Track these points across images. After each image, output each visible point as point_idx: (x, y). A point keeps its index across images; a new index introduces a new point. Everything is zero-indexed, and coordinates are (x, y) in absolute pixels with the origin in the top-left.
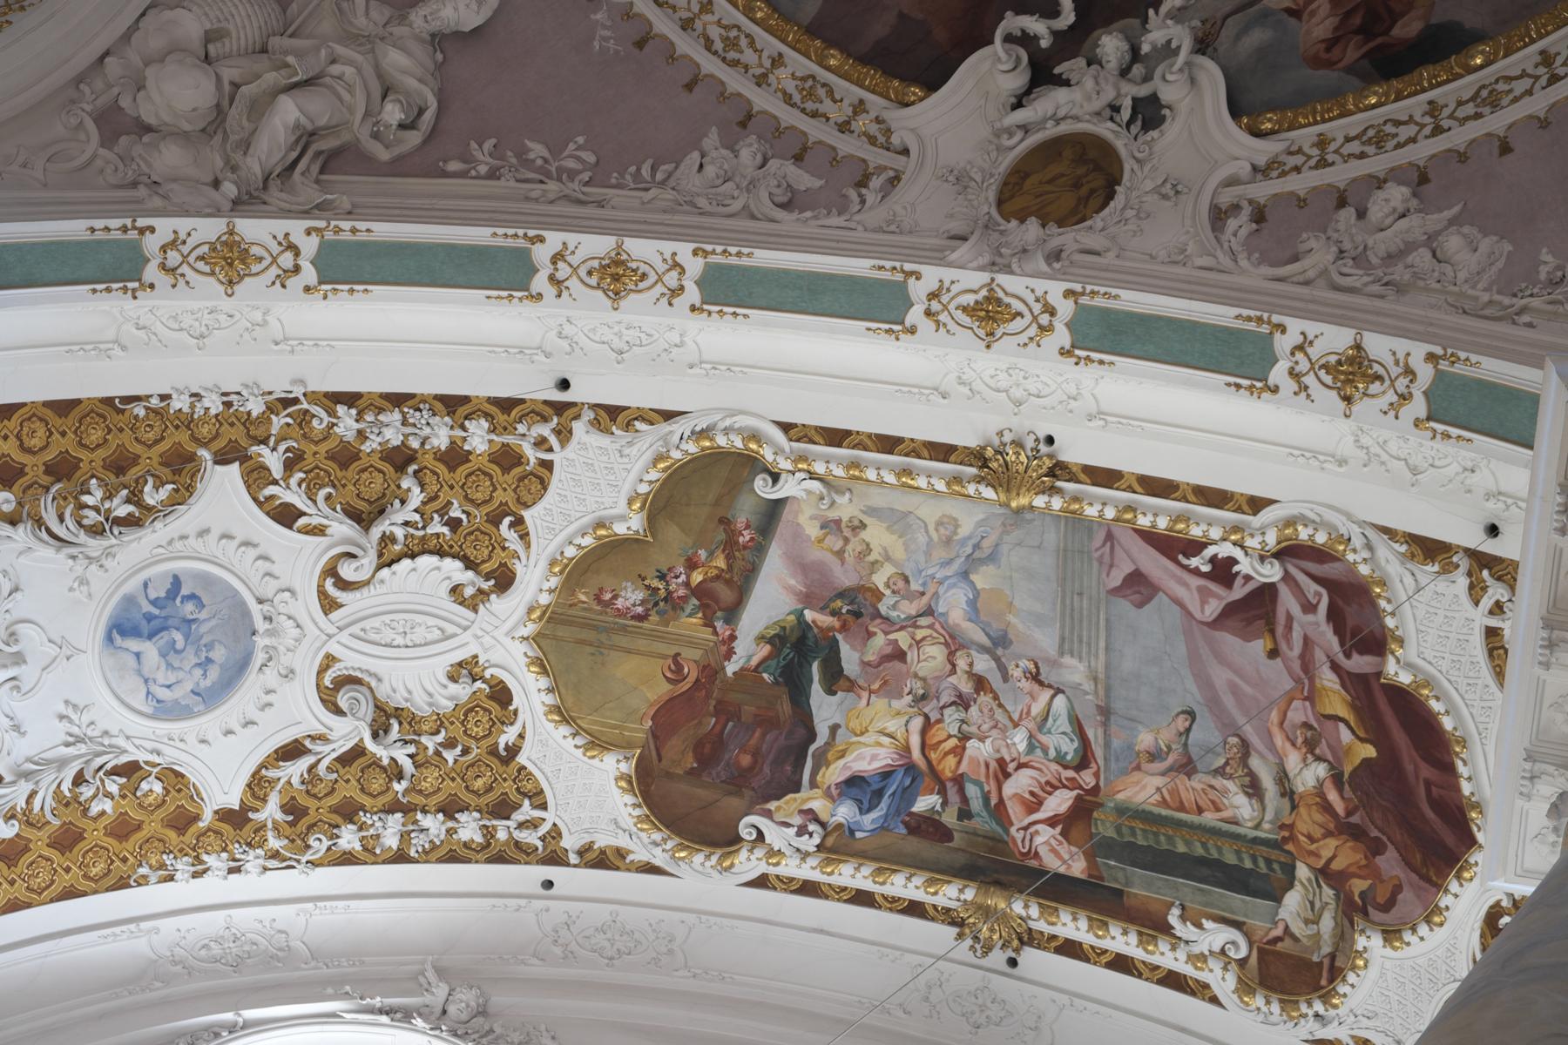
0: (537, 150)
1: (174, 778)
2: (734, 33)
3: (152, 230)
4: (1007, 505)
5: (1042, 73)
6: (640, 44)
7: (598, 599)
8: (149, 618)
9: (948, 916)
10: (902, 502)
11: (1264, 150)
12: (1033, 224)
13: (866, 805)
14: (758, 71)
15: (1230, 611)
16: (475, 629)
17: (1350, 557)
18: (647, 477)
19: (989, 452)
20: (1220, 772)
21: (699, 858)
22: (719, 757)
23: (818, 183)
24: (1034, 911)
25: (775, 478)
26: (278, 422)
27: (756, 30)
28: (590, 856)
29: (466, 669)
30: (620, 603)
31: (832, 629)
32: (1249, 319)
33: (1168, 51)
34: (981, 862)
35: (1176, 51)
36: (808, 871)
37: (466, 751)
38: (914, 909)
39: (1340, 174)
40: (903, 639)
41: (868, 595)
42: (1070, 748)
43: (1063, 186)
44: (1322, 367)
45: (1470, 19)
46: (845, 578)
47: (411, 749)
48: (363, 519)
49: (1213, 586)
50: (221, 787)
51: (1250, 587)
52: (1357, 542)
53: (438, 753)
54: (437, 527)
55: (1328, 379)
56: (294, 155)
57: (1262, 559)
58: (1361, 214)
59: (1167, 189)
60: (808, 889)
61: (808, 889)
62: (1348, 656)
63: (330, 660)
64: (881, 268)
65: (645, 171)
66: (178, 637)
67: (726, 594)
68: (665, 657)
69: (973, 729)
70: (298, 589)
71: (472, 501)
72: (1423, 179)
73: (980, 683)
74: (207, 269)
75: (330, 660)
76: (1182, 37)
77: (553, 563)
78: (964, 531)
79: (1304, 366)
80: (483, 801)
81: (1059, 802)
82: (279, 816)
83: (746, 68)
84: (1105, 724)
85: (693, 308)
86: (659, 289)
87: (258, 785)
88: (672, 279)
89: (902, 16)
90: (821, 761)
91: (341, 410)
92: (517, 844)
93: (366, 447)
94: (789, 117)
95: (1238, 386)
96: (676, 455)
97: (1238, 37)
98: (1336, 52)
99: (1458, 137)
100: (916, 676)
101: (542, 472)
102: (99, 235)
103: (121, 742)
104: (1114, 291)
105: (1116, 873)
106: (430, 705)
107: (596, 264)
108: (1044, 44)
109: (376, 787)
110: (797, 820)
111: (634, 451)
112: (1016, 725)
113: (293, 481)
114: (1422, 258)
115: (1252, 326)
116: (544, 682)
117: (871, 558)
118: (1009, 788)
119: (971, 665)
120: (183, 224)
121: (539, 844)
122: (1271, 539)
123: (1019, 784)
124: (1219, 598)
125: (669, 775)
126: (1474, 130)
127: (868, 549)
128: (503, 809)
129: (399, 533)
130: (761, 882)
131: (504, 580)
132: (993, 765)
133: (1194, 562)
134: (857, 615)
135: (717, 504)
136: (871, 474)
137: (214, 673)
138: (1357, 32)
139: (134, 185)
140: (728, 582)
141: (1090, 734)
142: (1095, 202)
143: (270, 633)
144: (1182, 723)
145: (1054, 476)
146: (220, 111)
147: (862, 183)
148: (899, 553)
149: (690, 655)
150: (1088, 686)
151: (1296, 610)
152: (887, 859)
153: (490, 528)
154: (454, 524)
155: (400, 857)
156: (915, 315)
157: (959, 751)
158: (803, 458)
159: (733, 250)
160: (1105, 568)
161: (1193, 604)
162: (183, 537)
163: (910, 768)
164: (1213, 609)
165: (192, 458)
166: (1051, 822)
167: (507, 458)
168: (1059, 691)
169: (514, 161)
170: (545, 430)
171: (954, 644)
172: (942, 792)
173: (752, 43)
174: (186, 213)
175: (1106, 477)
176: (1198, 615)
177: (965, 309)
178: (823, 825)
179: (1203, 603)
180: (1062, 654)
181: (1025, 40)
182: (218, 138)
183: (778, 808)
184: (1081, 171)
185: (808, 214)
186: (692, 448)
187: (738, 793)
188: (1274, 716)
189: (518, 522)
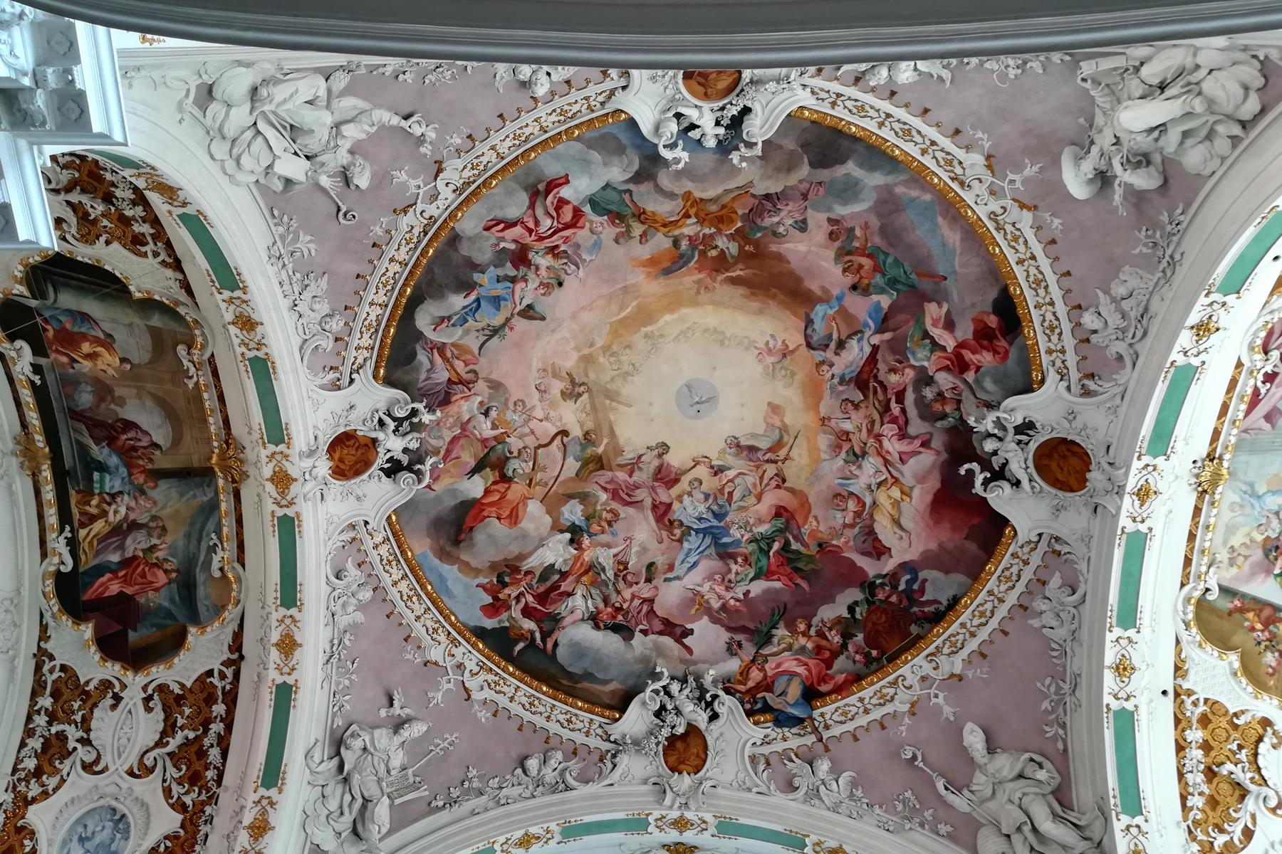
5: (1000, 475)
6: (984, 656)
7: (1272, 675)
10: (1221, 530)
11: (1052, 377)
12: (1088, 475)
23: (1058, 574)
25: (1208, 590)
26: (1201, 837)
27: (976, 603)
30: (1274, 664)
33: (999, 423)
35: (998, 418)
39: (1069, 342)
43: (1064, 464)
45: (993, 294)
46: (1258, 554)
48: (1244, 793)
54: (1243, 755)
59: (1071, 417)
67: (1267, 612)
76: (991, 417)
77: (1256, 698)
79: (1195, 351)
86: (1129, 648)
88: (1124, 642)
93: (1207, 791)
94: (1020, 587)
96: (1198, 638)
97: (988, 392)
101: (1210, 703)
113: (1230, 829)
114: (1126, 305)
115: (1169, 376)
127: (1244, 544)
129: (1249, 775)
131: (1266, 723)
135: (1221, 617)
138: (991, 342)
140: (1261, 611)
142: (1075, 449)
147: (1059, 554)
148: (1246, 530)
153: (1240, 729)
154: (1240, 747)
156: (1143, 528)
158: (1199, 577)
167: (1204, 721)
170: (1188, 702)
173: (982, 605)
177: (1142, 505)
181: (986, 483)
184: (1056, 456)
186: (1194, 630)
189: (1236, 715)
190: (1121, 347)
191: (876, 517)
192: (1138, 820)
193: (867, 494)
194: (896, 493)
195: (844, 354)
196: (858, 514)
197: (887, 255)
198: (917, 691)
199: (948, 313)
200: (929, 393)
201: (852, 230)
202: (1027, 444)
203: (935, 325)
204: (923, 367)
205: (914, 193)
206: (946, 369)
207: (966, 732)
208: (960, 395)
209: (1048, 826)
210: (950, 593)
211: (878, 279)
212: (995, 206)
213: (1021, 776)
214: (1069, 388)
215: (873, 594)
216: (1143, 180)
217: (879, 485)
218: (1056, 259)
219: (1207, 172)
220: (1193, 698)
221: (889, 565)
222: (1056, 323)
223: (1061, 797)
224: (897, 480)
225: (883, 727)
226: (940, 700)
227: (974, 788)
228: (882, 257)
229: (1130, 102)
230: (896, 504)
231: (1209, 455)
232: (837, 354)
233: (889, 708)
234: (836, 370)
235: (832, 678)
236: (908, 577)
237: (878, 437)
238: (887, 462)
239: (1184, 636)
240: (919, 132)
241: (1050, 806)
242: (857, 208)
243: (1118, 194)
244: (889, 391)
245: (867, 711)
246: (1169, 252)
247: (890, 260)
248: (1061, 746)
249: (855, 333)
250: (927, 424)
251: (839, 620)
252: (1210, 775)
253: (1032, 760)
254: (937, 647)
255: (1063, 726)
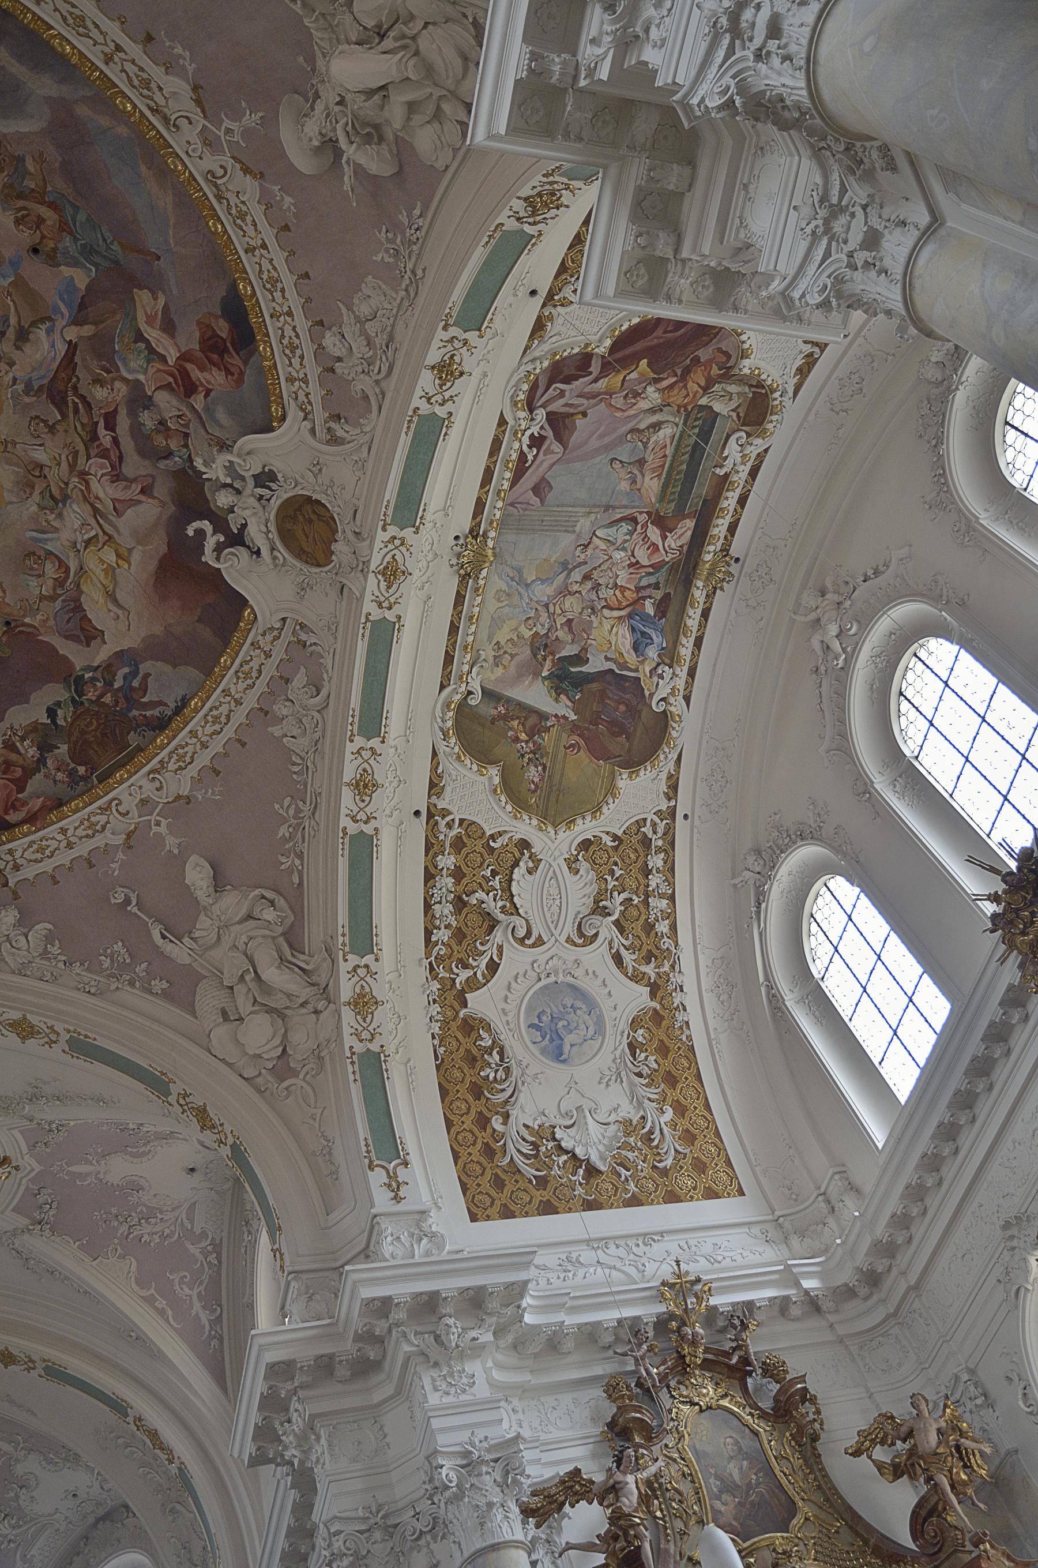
0: (283, 831)
1: (635, 1023)
2: (209, 718)
3: (351, 1047)
4: (492, 562)
5: (237, 539)
6: (217, 773)
7: (534, 792)
8: (552, 1040)
9: (710, 597)
10: (485, 622)
11: (293, 413)
13: (649, 641)
14: (233, 704)
15: (558, 437)
16: (550, 860)
17: (538, 371)
18: (469, 766)
19: (462, 572)
20: (645, 445)
21: (674, 734)
22: (622, 724)
23: (303, 670)
24: (712, 548)
25: (470, 693)
28: (671, 794)
29: (572, 864)
30: (536, 780)
31: (553, 661)
32: (408, 427)
33: (230, 469)
34: (683, 577)
36: (683, 673)
37: (616, 864)
38: (705, 614)
39: (313, 370)
40: (561, 620)
41: (535, 640)
42: (625, 527)
43: (309, 528)
44: (441, 386)
45: (221, 292)
47: (616, 893)
49: (544, 448)
50: (637, 998)
51: (547, 427)
52: (530, 367)
53: (617, 879)
54: (496, 883)
55: (449, 384)
56: (296, 969)
57: (532, 419)
58: (339, 359)
59: (315, 470)
60: (692, 673)
61: (692, 673)
62: (591, 373)
63: (569, 940)
64: (363, 636)
65: (296, 769)
66: (560, 1024)
67: (533, 720)
68: (566, 753)
69: (611, 581)
70: (531, 959)
71: (482, 864)
72: (321, 323)
73: (587, 577)
74: (370, 1016)
75: (569, 940)
76: (223, 458)
78: (504, 587)
79: (439, 398)
80: (642, 854)
81: (654, 533)
82: (652, 965)
83: (230, 711)
84: (614, 508)
85: (383, 742)
87: (637, 978)
88: (366, 754)
89: (199, 621)
90: (624, 666)
91: (434, 939)
92: (664, 834)
93: (454, 924)
94: (261, 686)
95: (446, 434)
97: (220, 426)
98: (232, 369)
99: (295, 302)
100: (581, 613)
101: (465, 825)
102: (358, 1077)
103: (618, 1053)
104: (385, 503)
105: (695, 502)
106: (591, 884)
107: (358, 798)
108: (222, 539)
109: (636, 913)
110: (655, 679)
111: (454, 773)
112: (611, 557)
114: (371, 328)
115: (413, 426)
116: (579, 821)
117: (516, 639)
118: (645, 562)
119: (577, 582)
120: (346, 1031)
121: (665, 822)
122: (522, 414)
123: (642, 556)
124: (551, 443)
125: (629, 750)
126: (291, 293)
128: (646, 842)
129: (500, 904)
130: (687, 699)
131: (524, 845)
132: (631, 570)
133: (530, 457)
134: (546, 646)
135: (483, 726)
136: (471, 639)
137: (578, 1004)
139: (320, 1058)
140: (526, 719)
141: (619, 516)
142: (321, 511)
143: (556, 974)
144: (617, 465)
145: (477, 535)
146: (270, 1010)
148: (514, 623)
149: (565, 739)
150: (593, 517)
151: (562, 401)
152: (678, 629)
154: (494, 873)
155: (672, 898)
156: (390, 616)
157: (623, 589)
158: (461, 677)
159: (350, 719)
160: (529, 507)
161: (552, 458)
162: (508, 1023)
163: (630, 616)
164: (557, 447)
165: (464, 1020)
166: (664, 538)
167: (458, 844)
168: (594, 533)
169: (291, 844)
171: (565, 591)
172: (644, 598)
174: (339, 1027)
175: (480, 506)
176: (559, 456)
177: (389, 587)
178: (658, 665)
179: (553, 452)
180: (575, 531)
181: (219, 549)
182: (287, 1012)
183: (648, 690)
185: (325, 676)
186: (453, 740)
187: (640, 712)
188: (618, 414)
189: (493, 837)
190: (364, 384)
191: (84, 588)
192: (369, 959)
193: (72, 554)
194: (111, 558)
195: (28, 348)
196: (60, 583)
197: (76, 208)
198: (135, 817)
199: (166, 308)
200: (147, 419)
201: (21, 159)
202: (268, 500)
203: (150, 321)
204: (137, 381)
205: (104, 121)
206: (167, 387)
207: (188, 867)
208: (187, 426)
209: (271, 974)
210: (180, 692)
211: (67, 241)
212: (210, 162)
213: (250, 917)
214: (313, 431)
215: (80, 693)
216: (374, 161)
217: (88, 542)
218: (292, 253)
219: (440, 165)
220: (448, 819)
221: (102, 655)
222: (296, 341)
223: (293, 938)
224: (110, 537)
225: (91, 866)
226: (163, 829)
227: (197, 934)
228: (69, 210)
229: (346, 47)
230: (110, 571)
231: (471, 531)
232: (18, 348)
233: (99, 841)
234: (17, 371)
235: (25, 803)
236: (126, 670)
237: (83, 475)
238: (96, 511)
239: (442, 748)
240: (97, 26)
241: (279, 950)
242: (23, 127)
243: (348, 171)
244: (95, 410)
245: (70, 846)
246: (410, 266)
247: (82, 217)
248: (296, 880)
249: (43, 320)
250: (147, 463)
251: (35, 728)
252: (460, 905)
253: (263, 897)
254: (161, 762)
255: (300, 856)
